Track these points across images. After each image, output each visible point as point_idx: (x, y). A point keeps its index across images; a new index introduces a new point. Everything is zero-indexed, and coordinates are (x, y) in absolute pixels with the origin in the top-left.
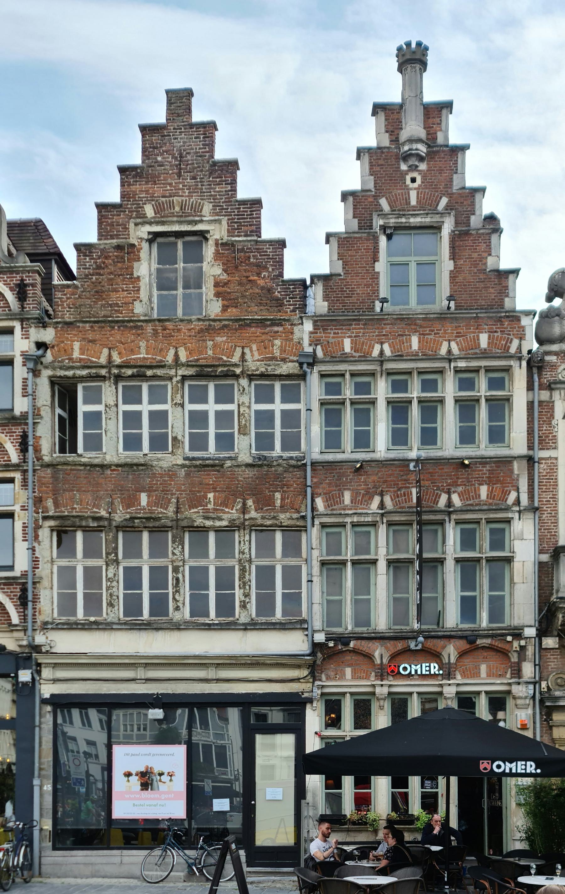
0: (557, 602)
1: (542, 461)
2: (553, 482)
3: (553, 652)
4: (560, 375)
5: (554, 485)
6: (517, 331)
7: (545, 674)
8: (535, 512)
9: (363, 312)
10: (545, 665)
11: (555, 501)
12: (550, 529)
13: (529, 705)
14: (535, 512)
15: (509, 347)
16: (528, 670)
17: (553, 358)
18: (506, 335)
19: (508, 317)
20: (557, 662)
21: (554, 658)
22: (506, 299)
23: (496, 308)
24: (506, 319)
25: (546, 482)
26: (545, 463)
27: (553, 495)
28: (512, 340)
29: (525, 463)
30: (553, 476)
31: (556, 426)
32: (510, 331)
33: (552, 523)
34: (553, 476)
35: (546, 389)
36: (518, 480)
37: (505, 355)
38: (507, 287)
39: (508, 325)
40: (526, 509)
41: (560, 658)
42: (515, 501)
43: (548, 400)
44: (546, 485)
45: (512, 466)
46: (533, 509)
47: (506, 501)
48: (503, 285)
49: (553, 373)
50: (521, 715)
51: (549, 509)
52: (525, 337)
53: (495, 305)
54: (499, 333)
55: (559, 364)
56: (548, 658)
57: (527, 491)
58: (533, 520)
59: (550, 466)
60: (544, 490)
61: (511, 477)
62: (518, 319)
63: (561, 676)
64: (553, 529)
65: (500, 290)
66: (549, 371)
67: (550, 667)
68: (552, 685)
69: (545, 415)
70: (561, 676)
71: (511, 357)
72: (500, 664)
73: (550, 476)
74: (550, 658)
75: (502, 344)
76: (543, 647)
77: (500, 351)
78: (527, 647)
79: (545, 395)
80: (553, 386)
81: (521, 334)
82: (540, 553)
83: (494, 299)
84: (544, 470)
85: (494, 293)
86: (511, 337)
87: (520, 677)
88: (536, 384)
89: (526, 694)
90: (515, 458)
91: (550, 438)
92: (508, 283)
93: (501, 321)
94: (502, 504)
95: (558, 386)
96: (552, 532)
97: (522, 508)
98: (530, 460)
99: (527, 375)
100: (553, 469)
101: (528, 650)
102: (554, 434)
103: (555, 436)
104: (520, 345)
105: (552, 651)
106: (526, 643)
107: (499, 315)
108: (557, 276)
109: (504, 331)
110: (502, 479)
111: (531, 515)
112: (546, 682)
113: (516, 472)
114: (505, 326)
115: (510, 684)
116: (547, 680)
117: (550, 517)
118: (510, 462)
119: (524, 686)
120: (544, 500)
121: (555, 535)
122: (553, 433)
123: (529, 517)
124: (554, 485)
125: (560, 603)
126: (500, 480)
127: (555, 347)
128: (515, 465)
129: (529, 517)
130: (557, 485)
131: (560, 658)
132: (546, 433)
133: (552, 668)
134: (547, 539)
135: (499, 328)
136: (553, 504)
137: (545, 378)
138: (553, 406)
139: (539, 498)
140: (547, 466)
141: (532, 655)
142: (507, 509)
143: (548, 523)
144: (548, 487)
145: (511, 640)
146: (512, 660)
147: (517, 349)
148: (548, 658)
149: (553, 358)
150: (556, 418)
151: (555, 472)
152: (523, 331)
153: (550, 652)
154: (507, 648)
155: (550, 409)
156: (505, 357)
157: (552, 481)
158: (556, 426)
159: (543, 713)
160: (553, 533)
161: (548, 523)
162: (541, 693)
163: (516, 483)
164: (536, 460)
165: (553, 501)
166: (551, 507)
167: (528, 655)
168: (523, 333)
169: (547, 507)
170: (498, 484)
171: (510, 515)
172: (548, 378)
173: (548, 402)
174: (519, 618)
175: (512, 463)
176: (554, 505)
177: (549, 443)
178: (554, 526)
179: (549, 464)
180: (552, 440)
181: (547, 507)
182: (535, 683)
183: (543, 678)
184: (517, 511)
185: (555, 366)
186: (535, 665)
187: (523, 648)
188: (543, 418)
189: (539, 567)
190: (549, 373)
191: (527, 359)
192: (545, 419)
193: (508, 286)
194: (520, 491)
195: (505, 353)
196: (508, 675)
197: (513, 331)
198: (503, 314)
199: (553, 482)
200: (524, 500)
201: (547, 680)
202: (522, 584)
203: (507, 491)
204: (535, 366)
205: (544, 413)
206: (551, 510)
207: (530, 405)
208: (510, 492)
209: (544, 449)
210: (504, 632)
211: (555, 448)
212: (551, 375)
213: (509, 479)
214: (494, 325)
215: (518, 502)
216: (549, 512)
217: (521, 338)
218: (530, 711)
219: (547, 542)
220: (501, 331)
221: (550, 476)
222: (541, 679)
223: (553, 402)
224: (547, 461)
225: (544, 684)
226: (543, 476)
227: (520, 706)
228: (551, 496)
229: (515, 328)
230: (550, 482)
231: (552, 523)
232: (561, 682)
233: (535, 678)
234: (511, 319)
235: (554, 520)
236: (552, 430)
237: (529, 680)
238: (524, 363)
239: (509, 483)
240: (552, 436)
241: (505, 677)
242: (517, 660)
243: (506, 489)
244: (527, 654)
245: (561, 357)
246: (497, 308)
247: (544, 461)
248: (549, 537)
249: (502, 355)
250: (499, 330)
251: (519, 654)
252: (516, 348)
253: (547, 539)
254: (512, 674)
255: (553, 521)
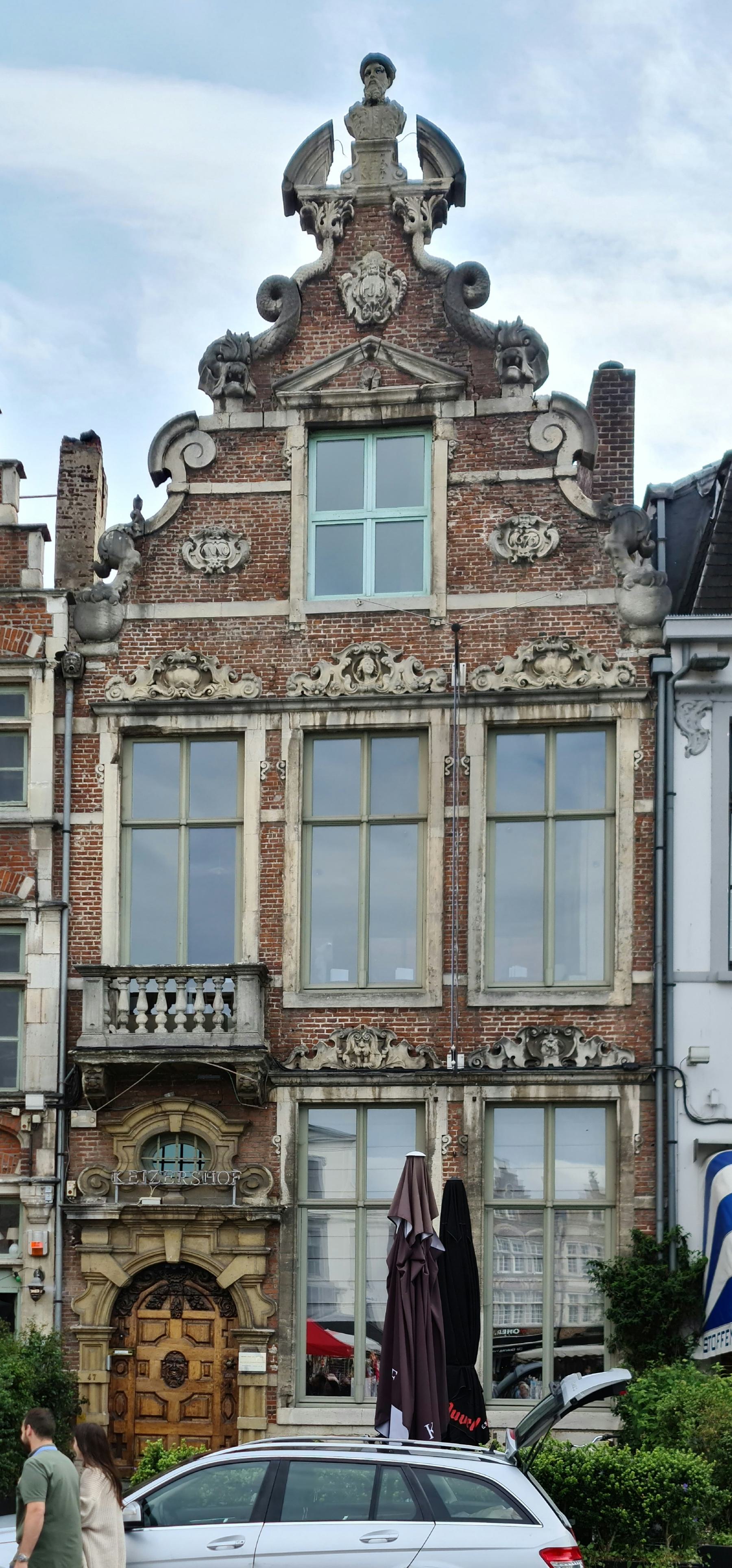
0: (74, 1055)
1: (79, 830)
2: (96, 864)
3: (89, 1134)
4: (108, 694)
5: (96, 869)
6: (39, 622)
7: (74, 1168)
8: (62, 912)
9: (469, 550)
10: (76, 1154)
11: (98, 894)
12: (89, 938)
13: (48, 1218)
14: (62, 912)
15: (26, 647)
16: (45, 1162)
17: (100, 666)
18: (22, 629)
19: (25, 599)
20: (95, 1149)
21: (90, 1144)
22: (24, 572)
23: (7, 586)
24: (22, 603)
25: (85, 864)
26: (84, 833)
27: (94, 883)
28: (31, 635)
29: (47, 832)
30: (96, 853)
31: (101, 774)
32: (28, 622)
33: (92, 928)
34: (96, 853)
35: (87, 716)
36: (36, 859)
37: (20, 659)
38: (25, 554)
39: (25, 612)
40: (49, 906)
41: (100, 1144)
42: (31, 892)
43: (90, 732)
44: (84, 869)
45: (28, 837)
46: (57, 905)
47: (17, 893)
48: (20, 549)
49: (100, 690)
50: (33, 1235)
51: (88, 907)
52: (51, 632)
53: (6, 581)
54: (12, 625)
55: (109, 675)
56: (81, 1144)
57: (50, 877)
58: (59, 923)
59: (91, 838)
60: (81, 876)
61: (25, 854)
62: (42, 604)
63: (98, 1172)
64: (94, 938)
65: (14, 557)
66: (93, 687)
67: (83, 1158)
68: (82, 1186)
69: (84, 756)
70: (98, 1172)
71: (27, 663)
72: (5, 1152)
73: (90, 854)
74: (84, 1144)
75: (16, 643)
76: (73, 1126)
77: (13, 653)
78: (45, 1125)
79: (84, 725)
80: (96, 710)
81: (46, 627)
82: (69, 975)
83: (5, 572)
84: (82, 844)
85: (5, 562)
86: (31, 631)
87: (32, 1173)
88: (69, 707)
89: (42, 1201)
90: (31, 824)
91: (93, 793)
92: (27, 547)
93: (14, 606)
94: (10, 897)
95: (104, 710)
96: (91, 943)
97: (40, 905)
98: (56, 828)
99: (56, 692)
100: (96, 843)
101: (45, 1129)
102: (99, 787)
103: (100, 790)
104: (44, 645)
105: (87, 1132)
106: (42, 1119)
107: (11, 597)
108: (107, 537)
109: (20, 622)
110: (11, 857)
111: (55, 916)
112: (74, 1182)
113: (33, 847)
114: (21, 614)
115: (16, 1184)
116: (76, 1179)
117: (90, 918)
118: (25, 831)
119: (39, 1188)
120: (81, 891)
121: (97, 948)
122: (96, 786)
123: (51, 919)
124: (96, 869)
125: (79, 1056)
126: (8, 859)
127: (102, 649)
128: (33, 835)
129: (51, 919)
130: (101, 869)
131: (100, 1144)
132: (85, 786)
133: (86, 1160)
134: (84, 953)
135: (10, 617)
136: (94, 899)
137: (87, 697)
138: (98, 742)
139: (70, 888)
140: (87, 838)
141: (52, 1138)
142: (17, 905)
143: (86, 928)
144: (88, 871)
145: (18, 1114)
146: (22, 1146)
147: (40, 650)
148: (81, 1144)
149: (100, 666)
150: (101, 762)
151: (100, 848)
152: (50, 622)
153: (84, 1134)
154: (12, 1127)
155: (93, 747)
156: (19, 663)
157: (93, 861)
158: (101, 774)
159: (71, 1232)
160: (94, 945)
161: (86, 928)
162: (66, 1199)
163: (33, 864)
164: (67, 827)
165: (95, 894)
166: (91, 904)
167: (46, 1139)
168: (49, 625)
169: (84, 904)
170: (4, 865)
171: (23, 915)
172: (91, 697)
173: (90, 736)
174: (33, 1080)
175: (28, 832)
176: (96, 900)
177: (91, 801)
178: (96, 934)
179: (90, 835)
180: (95, 796)
181: (84, 904)
182: (55, 1184)
183: (72, 1175)
184: (33, 909)
185: (102, 678)
186: (57, 1155)
187: (37, 1128)
188: (82, 761)
189: (67, 999)
190: (92, 690)
191: (54, 666)
192: (85, 763)
193: (26, 552)
194: (39, 877)
195: (19, 656)
196: (18, 1170)
197: (33, 622)
198: (18, 596)
199: (96, 864)
200: (46, 892)
201: (76, 1179)
202: (38, 1025)
203: (19, 876)
204: (69, 678)
205: (84, 753)
206: (91, 909)
207: (58, 740)
208: (23, 878)
209: (81, 811)
210: (8, 1100)
211: (100, 810)
212: (95, 692)
213: (22, 857)
214: (4, 612)
215: (35, 895)
216: (88, 910)
217: (46, 633)
218: (50, 1228)
219: (83, 958)
220: (14, 622)
221: (90, 854)
222: (67, 1177)
223: (98, 736)
224: (87, 831)
225: (70, 1185)
226: (79, 853)
227: (34, 1220)
228: (92, 886)
229: (37, 617)
230: (91, 864)
231: (92, 928)
232: (96, 1181)
233: (56, 1175)
234: (31, 603)
235: (96, 923)
236: (96, 781)
237: (44, 1178)
238: (50, 674)
239: (22, 864)
240: (95, 791)
241: (13, 1172)
242: (28, 1147)
243: (17, 873)
244: (44, 1136)
245: (113, 664)
246: (9, 586)
247: (81, 831)
248: (87, 951)
249: (14, 660)
250: (10, 620)
251: (31, 1136)
252: (37, 649)
253: (84, 953)
254: (22, 1168)
255: (94, 925)
